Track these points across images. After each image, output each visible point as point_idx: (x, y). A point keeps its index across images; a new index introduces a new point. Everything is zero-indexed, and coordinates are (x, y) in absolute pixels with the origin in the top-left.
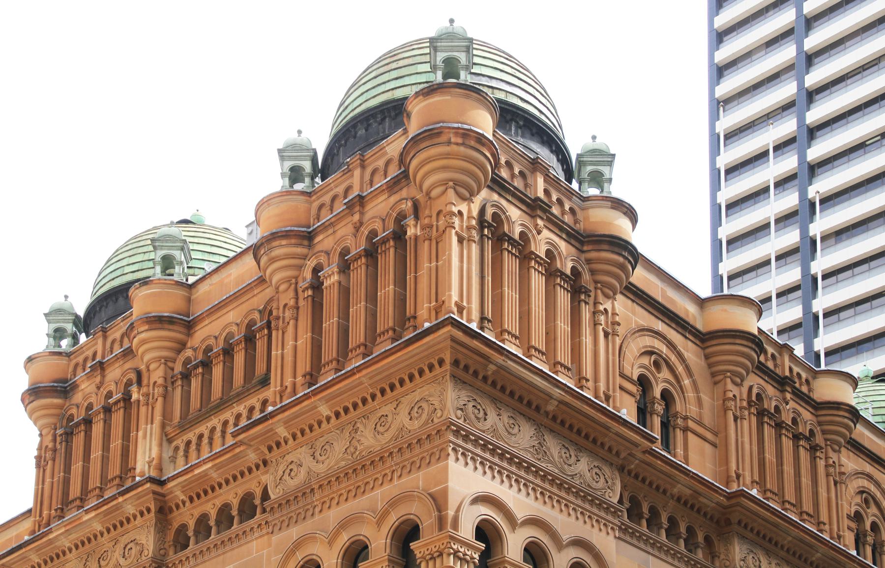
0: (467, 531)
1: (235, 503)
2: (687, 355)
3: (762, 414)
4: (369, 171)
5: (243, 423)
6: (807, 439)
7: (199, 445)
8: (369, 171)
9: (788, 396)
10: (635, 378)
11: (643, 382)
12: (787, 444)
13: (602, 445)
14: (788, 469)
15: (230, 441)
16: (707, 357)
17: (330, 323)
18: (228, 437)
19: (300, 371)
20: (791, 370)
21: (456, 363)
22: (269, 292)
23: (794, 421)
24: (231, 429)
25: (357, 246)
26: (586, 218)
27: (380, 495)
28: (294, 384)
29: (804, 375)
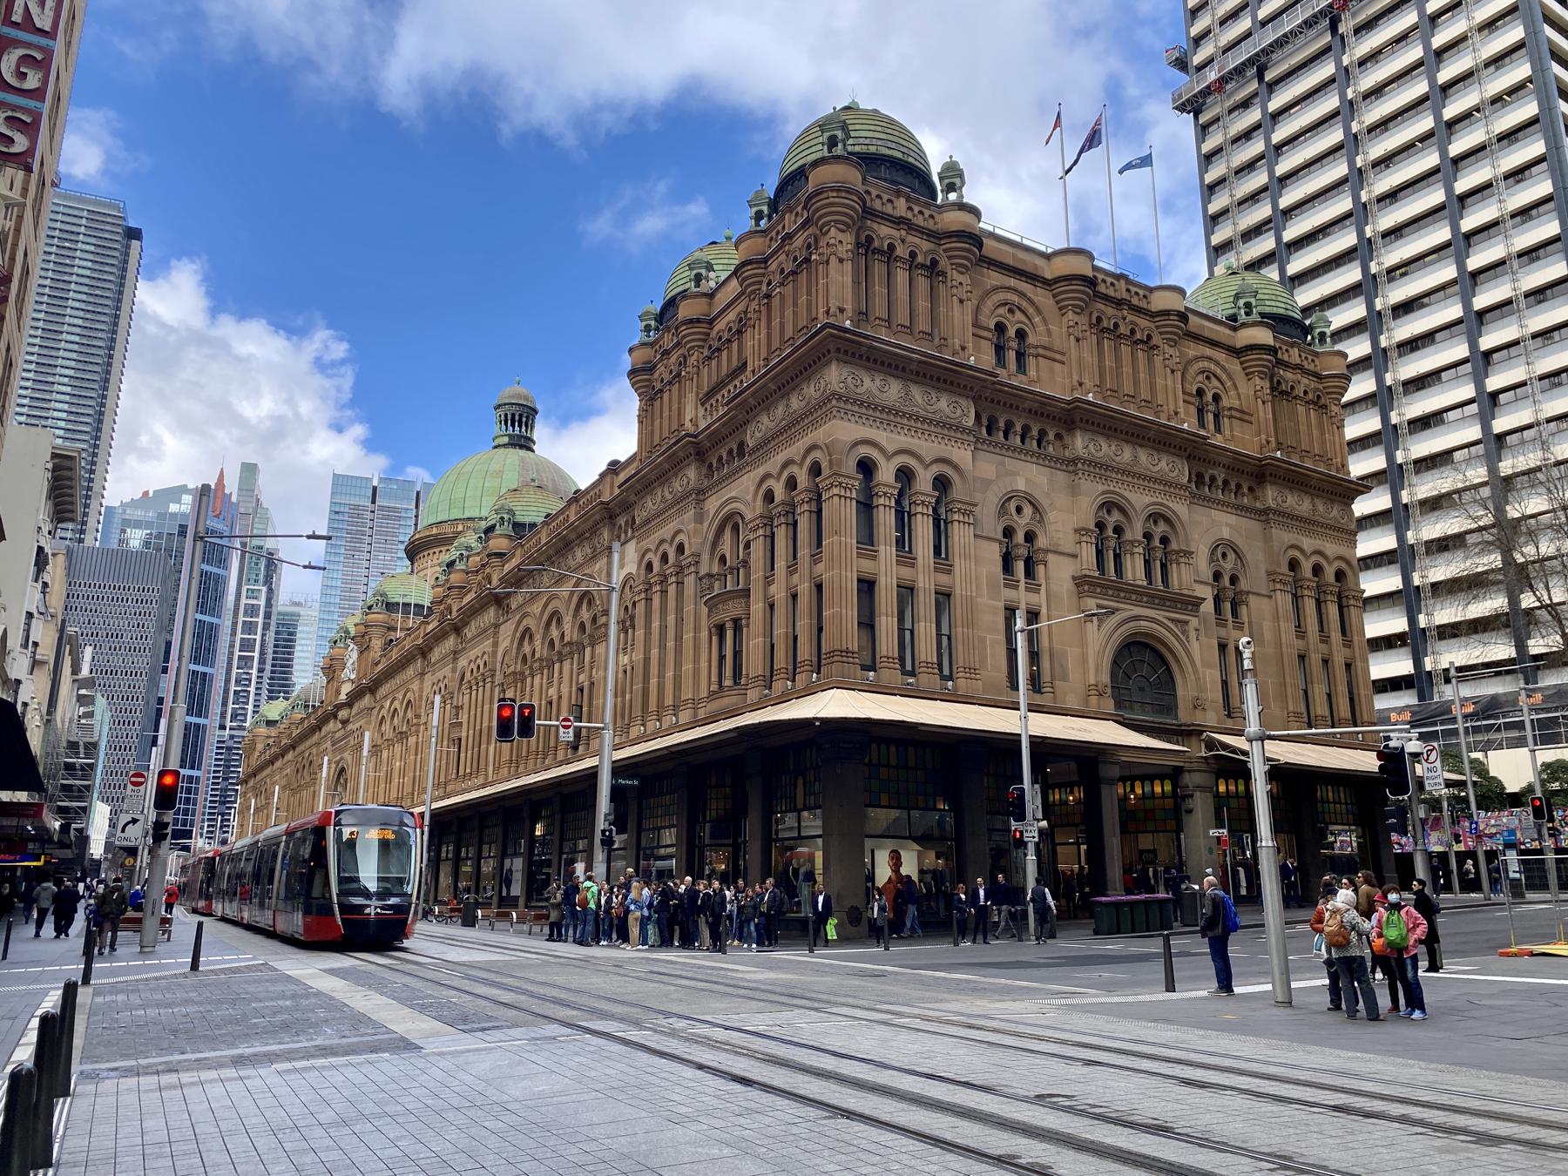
0: (850, 466)
2: (1035, 299)
9: (1125, 312)
13: (959, 385)
16: (1054, 296)
29: (1141, 292)
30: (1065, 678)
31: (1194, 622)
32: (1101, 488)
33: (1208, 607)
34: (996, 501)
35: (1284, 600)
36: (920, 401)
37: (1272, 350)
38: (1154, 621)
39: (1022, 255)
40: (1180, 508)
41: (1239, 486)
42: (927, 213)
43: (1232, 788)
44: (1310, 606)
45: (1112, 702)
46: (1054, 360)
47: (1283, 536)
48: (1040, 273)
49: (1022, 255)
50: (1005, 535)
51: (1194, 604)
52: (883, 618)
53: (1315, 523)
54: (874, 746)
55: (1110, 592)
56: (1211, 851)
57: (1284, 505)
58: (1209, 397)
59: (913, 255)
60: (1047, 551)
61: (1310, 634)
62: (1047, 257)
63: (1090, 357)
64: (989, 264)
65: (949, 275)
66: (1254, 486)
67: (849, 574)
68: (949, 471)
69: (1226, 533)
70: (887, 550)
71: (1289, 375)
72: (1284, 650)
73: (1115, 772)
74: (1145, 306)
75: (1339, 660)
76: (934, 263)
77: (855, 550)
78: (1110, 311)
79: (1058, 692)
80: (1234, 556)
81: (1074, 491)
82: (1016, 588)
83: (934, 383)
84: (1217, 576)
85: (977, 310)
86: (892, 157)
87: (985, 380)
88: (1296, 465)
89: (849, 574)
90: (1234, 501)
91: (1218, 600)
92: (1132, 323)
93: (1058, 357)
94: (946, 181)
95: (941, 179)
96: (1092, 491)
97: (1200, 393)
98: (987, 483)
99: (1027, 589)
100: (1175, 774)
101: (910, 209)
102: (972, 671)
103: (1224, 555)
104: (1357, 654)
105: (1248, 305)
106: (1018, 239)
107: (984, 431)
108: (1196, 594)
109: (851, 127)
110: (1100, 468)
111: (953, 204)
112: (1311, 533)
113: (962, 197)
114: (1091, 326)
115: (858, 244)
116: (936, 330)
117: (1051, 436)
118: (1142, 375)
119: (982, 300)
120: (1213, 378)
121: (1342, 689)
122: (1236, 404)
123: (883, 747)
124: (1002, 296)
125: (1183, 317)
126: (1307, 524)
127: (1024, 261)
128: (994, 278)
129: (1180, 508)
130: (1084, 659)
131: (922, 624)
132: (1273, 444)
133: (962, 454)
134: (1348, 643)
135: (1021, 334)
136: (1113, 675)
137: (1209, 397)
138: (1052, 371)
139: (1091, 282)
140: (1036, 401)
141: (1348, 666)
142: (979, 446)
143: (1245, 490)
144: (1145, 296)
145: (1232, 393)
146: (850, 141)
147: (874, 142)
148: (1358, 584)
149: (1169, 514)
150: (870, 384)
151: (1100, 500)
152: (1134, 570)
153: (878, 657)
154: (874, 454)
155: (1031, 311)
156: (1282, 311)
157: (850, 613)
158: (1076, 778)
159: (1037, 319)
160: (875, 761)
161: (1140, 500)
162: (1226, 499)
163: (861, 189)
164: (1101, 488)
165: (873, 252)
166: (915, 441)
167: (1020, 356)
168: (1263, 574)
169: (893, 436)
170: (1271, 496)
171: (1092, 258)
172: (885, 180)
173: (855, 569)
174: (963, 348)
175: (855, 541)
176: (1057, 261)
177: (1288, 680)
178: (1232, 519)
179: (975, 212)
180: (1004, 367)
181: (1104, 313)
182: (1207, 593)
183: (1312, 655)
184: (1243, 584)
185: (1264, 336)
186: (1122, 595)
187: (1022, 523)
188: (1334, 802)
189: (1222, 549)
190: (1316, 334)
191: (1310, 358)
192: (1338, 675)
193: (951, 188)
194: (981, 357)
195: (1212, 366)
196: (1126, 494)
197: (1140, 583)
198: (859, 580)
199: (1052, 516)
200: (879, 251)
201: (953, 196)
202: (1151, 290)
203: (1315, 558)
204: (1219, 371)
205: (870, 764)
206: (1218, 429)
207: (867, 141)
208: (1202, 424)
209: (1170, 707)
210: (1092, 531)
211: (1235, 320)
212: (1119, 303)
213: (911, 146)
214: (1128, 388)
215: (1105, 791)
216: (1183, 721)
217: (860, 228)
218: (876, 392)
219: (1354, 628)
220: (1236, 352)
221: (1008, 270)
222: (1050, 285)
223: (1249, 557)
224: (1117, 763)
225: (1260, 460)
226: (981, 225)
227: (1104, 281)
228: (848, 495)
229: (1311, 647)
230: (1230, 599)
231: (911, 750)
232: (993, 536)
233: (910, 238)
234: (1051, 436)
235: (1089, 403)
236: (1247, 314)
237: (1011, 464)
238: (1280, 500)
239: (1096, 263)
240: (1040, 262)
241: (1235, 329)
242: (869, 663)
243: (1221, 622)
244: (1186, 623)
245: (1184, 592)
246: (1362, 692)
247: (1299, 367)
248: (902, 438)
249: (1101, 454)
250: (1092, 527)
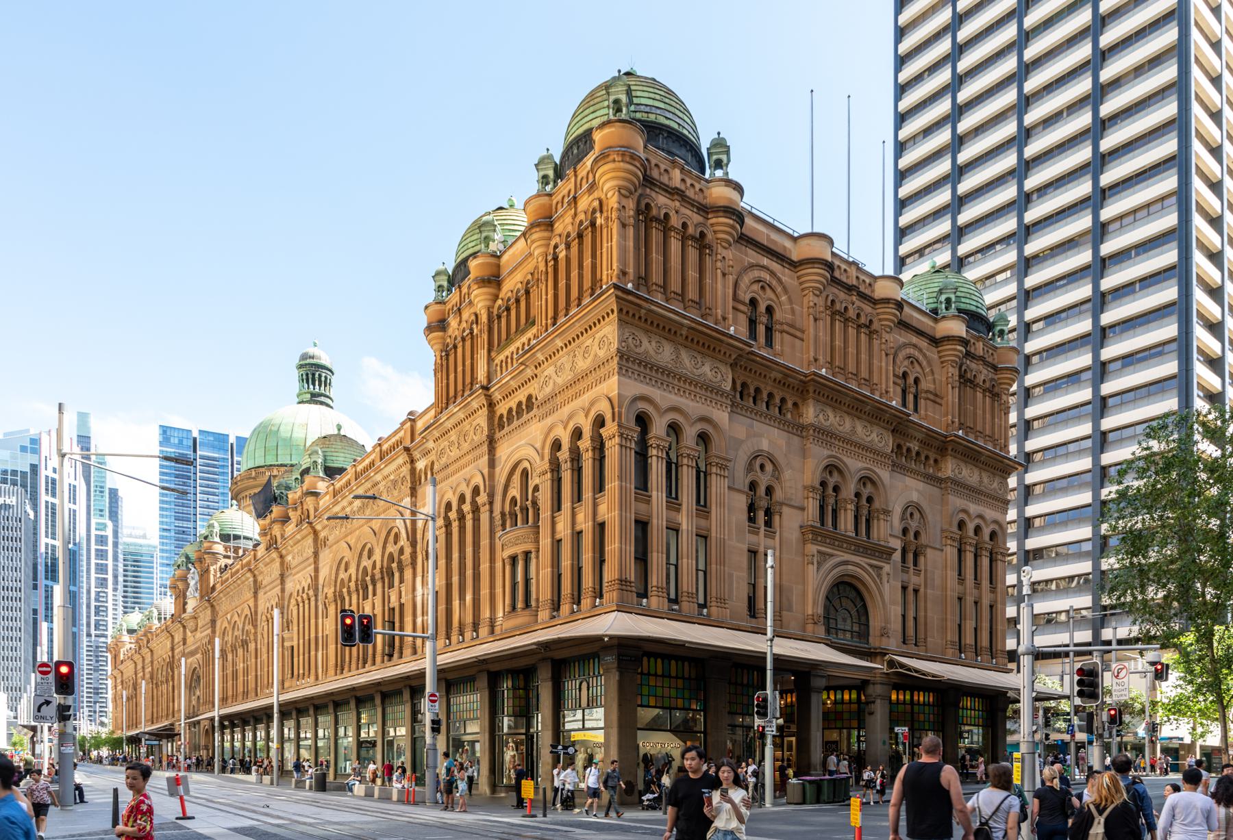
2: (784, 279)
3: (834, 314)
5: (521, 352)
6: (868, 327)
9: (854, 298)
10: (747, 301)
11: (753, 302)
12: (852, 331)
14: (852, 350)
17: (562, 283)
18: (515, 361)
19: (549, 316)
20: (857, 278)
21: (620, 311)
23: (858, 315)
24: (515, 356)
26: (711, 194)
28: (547, 324)
29: (868, 281)
30: (790, 609)
31: (887, 568)
32: (826, 452)
33: (897, 556)
34: (746, 458)
35: (951, 552)
36: (688, 364)
37: (964, 342)
38: (858, 565)
39: (774, 236)
40: (884, 474)
41: (927, 458)
42: (698, 186)
43: (901, 697)
44: (969, 558)
45: (823, 628)
46: (796, 337)
47: (956, 501)
48: (788, 256)
49: (774, 236)
50: (751, 490)
51: (886, 553)
52: (655, 554)
53: (980, 492)
54: (645, 659)
55: (828, 541)
56: (884, 743)
57: (959, 476)
58: (911, 380)
59: (684, 225)
60: (781, 504)
61: (968, 582)
62: (795, 239)
63: (824, 336)
64: (747, 241)
65: (714, 249)
66: (939, 457)
67: (628, 514)
68: (710, 429)
69: (915, 497)
70: (658, 495)
71: (973, 366)
72: (949, 593)
73: (822, 683)
74: (869, 294)
75: (985, 602)
76: (702, 235)
77: (633, 495)
78: (842, 295)
79: (784, 620)
80: (919, 515)
81: (804, 453)
82: (757, 534)
83: (700, 349)
84: (905, 531)
85: (736, 285)
86: (669, 127)
87: (741, 349)
88: (973, 443)
89: (628, 514)
90: (923, 470)
91: (904, 551)
92: (859, 308)
93: (798, 334)
94: (715, 157)
95: (709, 155)
96: (819, 454)
97: (905, 375)
98: (740, 443)
99: (766, 536)
100: (862, 686)
101: (683, 180)
102: (722, 601)
103: (912, 514)
104: (999, 599)
105: (948, 301)
106: (771, 221)
107: (738, 396)
108: (890, 545)
109: (634, 94)
110: (825, 435)
111: (721, 180)
112: (977, 501)
113: (727, 174)
114: (826, 308)
115: (638, 212)
116: (703, 300)
117: (790, 404)
118: (863, 356)
119: (739, 275)
120: (916, 364)
121: (985, 625)
122: (931, 387)
123: (652, 660)
124: (756, 273)
125: (900, 305)
126: (974, 492)
127: (775, 242)
128: (752, 256)
129: (884, 474)
130: (804, 594)
131: (685, 560)
132: (957, 424)
133: (721, 416)
134: (993, 589)
135: (769, 310)
136: (826, 608)
137: (911, 380)
138: (793, 347)
139: (830, 266)
140: (781, 372)
141: (991, 607)
142: (734, 409)
143: (932, 462)
144: (870, 285)
145: (930, 378)
146: (632, 108)
147: (654, 110)
148: (1005, 543)
149: (875, 478)
150: (648, 344)
151: (825, 463)
152: (846, 522)
153: (649, 586)
154: (650, 409)
155: (779, 289)
156: (973, 308)
157: (628, 548)
158: (792, 687)
159: (784, 298)
160: (645, 671)
161: (855, 465)
162: (917, 468)
163: (643, 156)
164: (826, 452)
165: (651, 220)
166: (682, 400)
167: (769, 330)
168: (938, 532)
169: (666, 394)
170: (949, 468)
171: (831, 242)
172: (663, 150)
173: (633, 511)
174: (724, 319)
175: (633, 487)
176: (803, 242)
177: (949, 617)
178: (921, 485)
179: (739, 188)
180: (755, 339)
181: (837, 297)
182: (897, 544)
183: (968, 598)
184: (923, 539)
185: (958, 328)
186: (837, 543)
187: (764, 481)
188: (971, 709)
189: (911, 510)
190: (996, 332)
191: (991, 351)
192: (984, 614)
193: (719, 164)
194: (737, 328)
195: (916, 353)
196: (845, 459)
197: (850, 534)
198: (637, 521)
199: (787, 474)
200: (657, 220)
201: (719, 173)
202: (875, 278)
203: (977, 521)
204: (921, 358)
205: (642, 673)
206: (916, 410)
207: (647, 109)
208: (904, 405)
209: (864, 634)
210: (818, 489)
211: (937, 314)
212: (849, 288)
213: (686, 118)
214: (851, 367)
215: (814, 698)
216: (872, 645)
217: (641, 195)
218: (652, 353)
219: (999, 578)
220: (935, 341)
221: (763, 250)
222: (795, 267)
223: (930, 517)
224: (823, 677)
225: (946, 437)
226: (742, 204)
227: (839, 267)
228: (628, 445)
229: (968, 591)
230: (913, 553)
231: (673, 662)
232: (742, 488)
233: (684, 210)
234: (790, 404)
235: (821, 376)
236: (947, 309)
237: (758, 426)
238: (957, 471)
239: (834, 250)
240: (788, 244)
241: (936, 321)
242: (642, 592)
243: (905, 569)
244: (881, 568)
245: (882, 543)
246: (999, 627)
247: (982, 359)
248: (673, 397)
249: (828, 423)
250: (818, 486)
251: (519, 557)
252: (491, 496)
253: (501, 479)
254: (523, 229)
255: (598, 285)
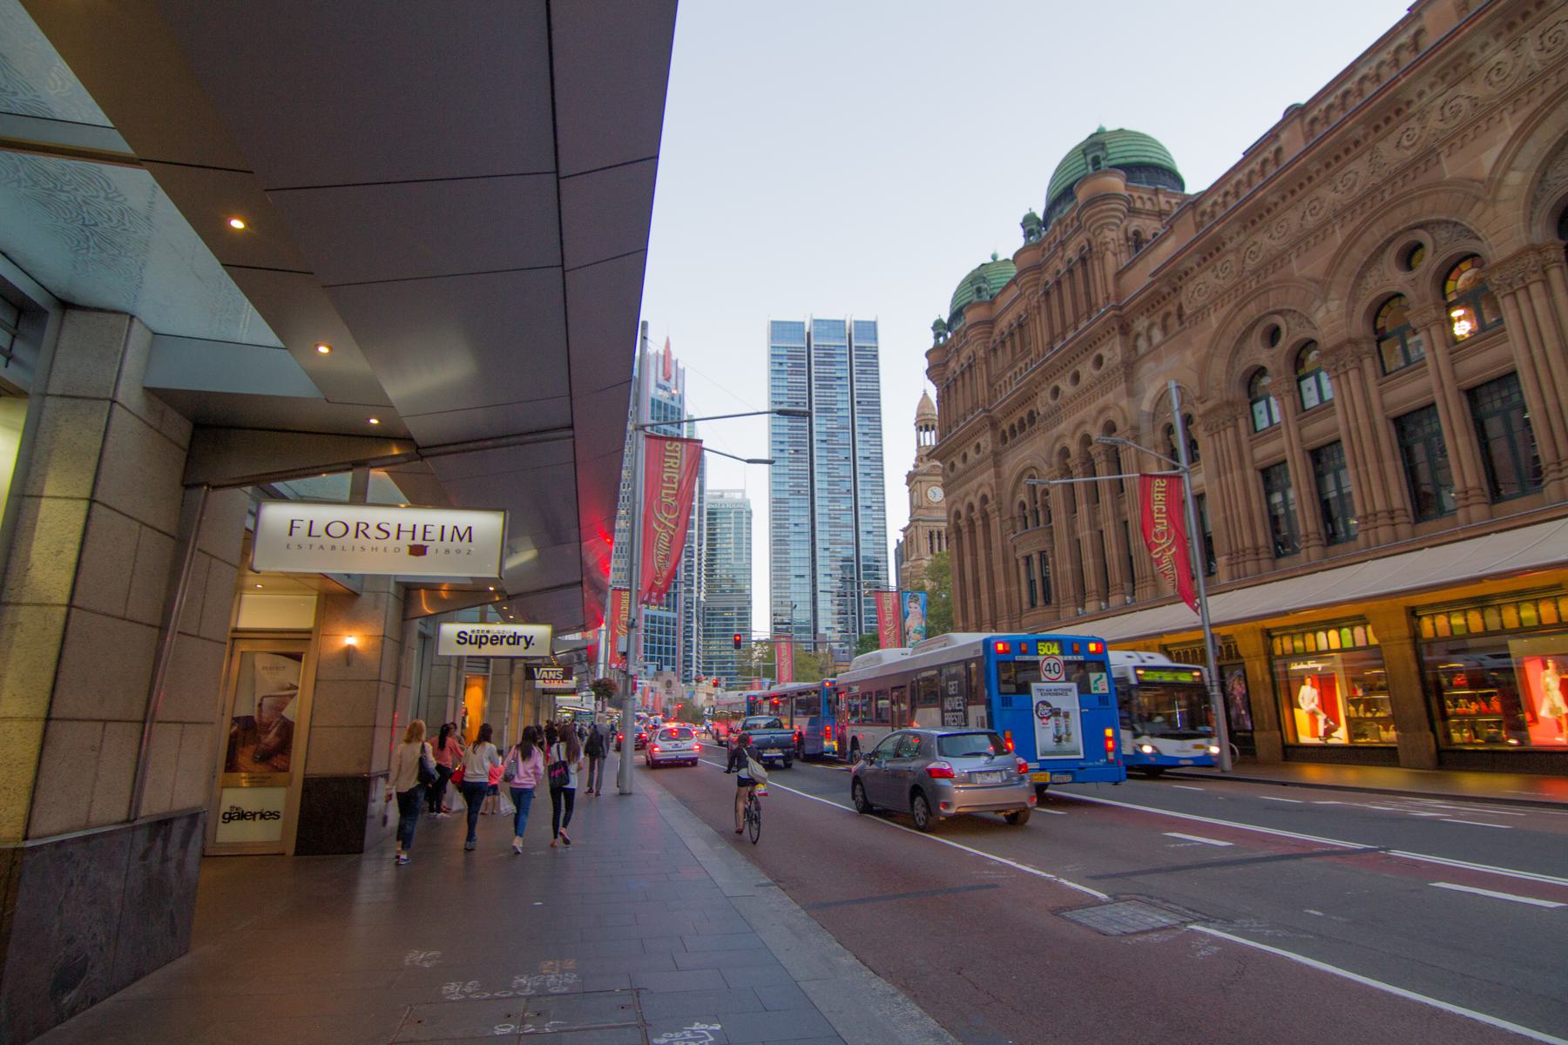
1: (1016, 423)
4: (1064, 225)
7: (1005, 387)
8: (1064, 225)
15: (1014, 389)
22: (1025, 301)
25: (1063, 269)
27: (1092, 409)
251: (1034, 556)
252: (1000, 503)
253: (1009, 486)
254: (1013, 275)
255: (1094, 309)
